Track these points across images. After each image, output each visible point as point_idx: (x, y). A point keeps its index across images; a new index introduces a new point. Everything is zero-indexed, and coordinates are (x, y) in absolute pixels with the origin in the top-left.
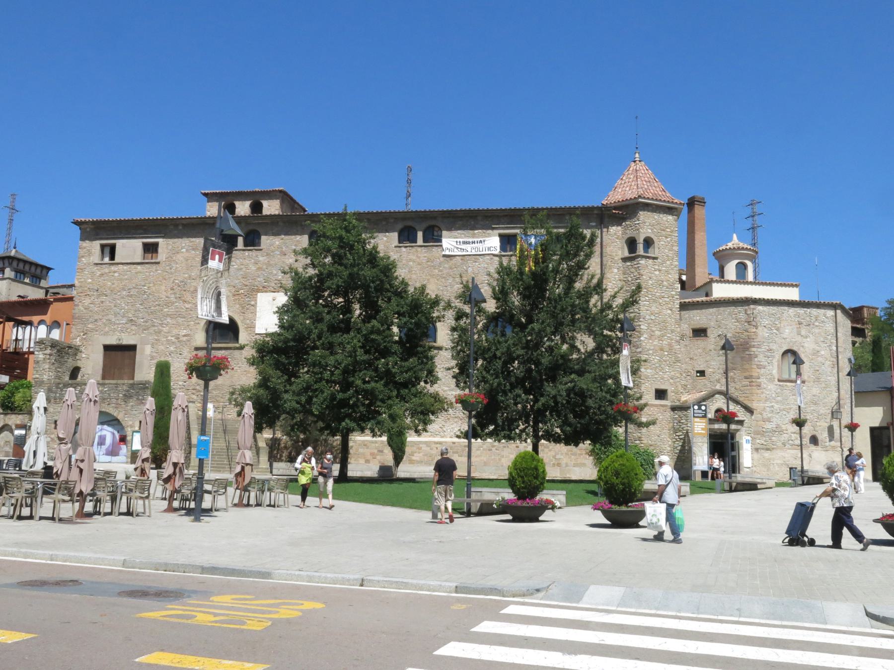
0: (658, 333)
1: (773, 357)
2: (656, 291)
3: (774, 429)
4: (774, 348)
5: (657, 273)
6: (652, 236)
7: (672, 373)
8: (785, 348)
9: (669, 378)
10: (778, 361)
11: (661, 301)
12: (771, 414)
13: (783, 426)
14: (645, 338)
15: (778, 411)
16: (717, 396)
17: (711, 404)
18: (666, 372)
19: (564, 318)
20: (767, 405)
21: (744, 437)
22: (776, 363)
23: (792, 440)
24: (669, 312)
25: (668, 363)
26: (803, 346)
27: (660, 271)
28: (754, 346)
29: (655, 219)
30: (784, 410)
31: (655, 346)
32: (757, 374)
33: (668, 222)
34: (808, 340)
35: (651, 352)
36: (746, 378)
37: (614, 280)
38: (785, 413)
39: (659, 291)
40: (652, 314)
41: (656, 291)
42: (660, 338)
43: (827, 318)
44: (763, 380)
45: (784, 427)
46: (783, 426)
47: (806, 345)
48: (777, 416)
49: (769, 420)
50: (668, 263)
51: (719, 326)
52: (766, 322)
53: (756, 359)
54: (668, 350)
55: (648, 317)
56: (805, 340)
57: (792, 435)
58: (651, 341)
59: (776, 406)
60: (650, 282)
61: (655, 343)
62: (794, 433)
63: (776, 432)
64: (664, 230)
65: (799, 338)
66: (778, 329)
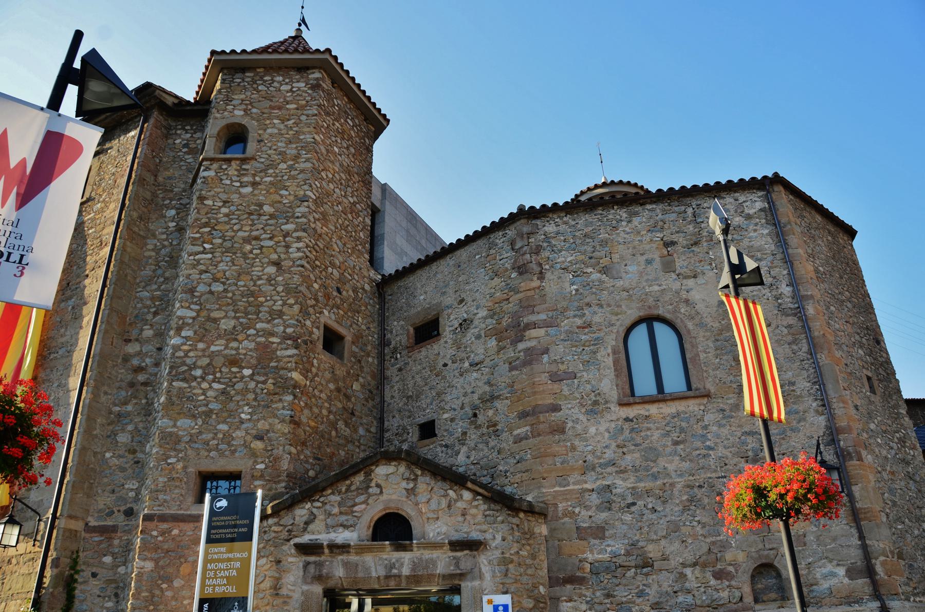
0: (226, 324)
1: (598, 341)
2: (236, 228)
3: (621, 560)
4: (597, 319)
5: (249, 189)
6: (245, 121)
7: (262, 425)
8: (633, 314)
9: (249, 438)
10: (615, 352)
11: (248, 247)
12: (604, 515)
13: (650, 547)
14: (183, 337)
15: (630, 500)
16: (381, 471)
17: (362, 498)
18: (242, 422)
19: (615, 452)
20: (588, 486)
21: (485, 598)
22: (609, 361)
23: (689, 592)
24: (271, 270)
25: (251, 396)
26: (687, 301)
27: (254, 184)
28: (534, 325)
29: (259, 91)
30: (648, 492)
31: (212, 356)
32: (549, 401)
33: (294, 92)
34: (700, 280)
35: (198, 372)
36: (523, 415)
37: (163, 233)
38: (651, 502)
39: (247, 228)
40: (216, 280)
41: (236, 228)
42: (231, 336)
43: (749, 217)
44: (572, 412)
45: (652, 551)
46: (650, 547)
47: (695, 296)
48: (628, 517)
49: (599, 532)
50: (283, 166)
51: (462, 301)
52: (567, 257)
53: (545, 358)
54: (254, 362)
55: (201, 288)
56: (690, 283)
57: (688, 571)
58: (201, 346)
59: (621, 485)
60: (225, 210)
61: (213, 348)
62: (695, 565)
63: (628, 568)
64: (280, 108)
65: (671, 282)
66: (605, 270)
